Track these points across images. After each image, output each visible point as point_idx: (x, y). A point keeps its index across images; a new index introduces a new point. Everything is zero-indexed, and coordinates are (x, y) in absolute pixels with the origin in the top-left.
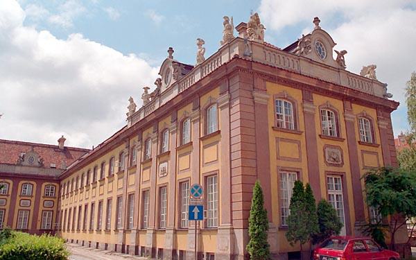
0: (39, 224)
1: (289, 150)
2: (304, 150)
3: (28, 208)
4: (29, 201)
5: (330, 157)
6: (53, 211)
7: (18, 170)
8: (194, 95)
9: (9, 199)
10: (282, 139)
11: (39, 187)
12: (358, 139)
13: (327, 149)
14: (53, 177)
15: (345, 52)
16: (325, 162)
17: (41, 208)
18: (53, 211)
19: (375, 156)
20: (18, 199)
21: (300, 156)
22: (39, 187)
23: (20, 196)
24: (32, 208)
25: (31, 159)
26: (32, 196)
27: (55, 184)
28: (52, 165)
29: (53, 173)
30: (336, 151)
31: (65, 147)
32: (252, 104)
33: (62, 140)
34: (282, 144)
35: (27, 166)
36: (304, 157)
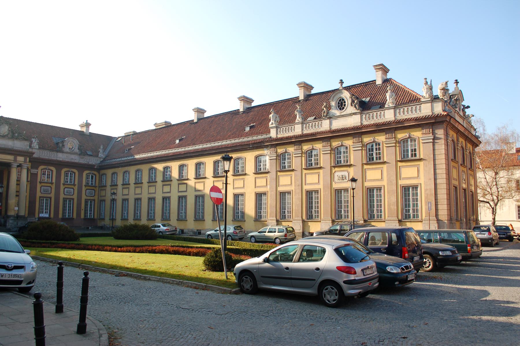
0: (83, 213)
4: (72, 190)
6: (94, 200)
7: (61, 157)
9: (54, 186)
11: (81, 176)
14: (94, 166)
15: (468, 107)
17: (84, 197)
18: (94, 200)
20: (62, 187)
22: (81, 176)
23: (64, 184)
24: (75, 197)
26: (74, 185)
27: (95, 173)
29: (93, 161)
31: (90, 133)
35: (67, 153)
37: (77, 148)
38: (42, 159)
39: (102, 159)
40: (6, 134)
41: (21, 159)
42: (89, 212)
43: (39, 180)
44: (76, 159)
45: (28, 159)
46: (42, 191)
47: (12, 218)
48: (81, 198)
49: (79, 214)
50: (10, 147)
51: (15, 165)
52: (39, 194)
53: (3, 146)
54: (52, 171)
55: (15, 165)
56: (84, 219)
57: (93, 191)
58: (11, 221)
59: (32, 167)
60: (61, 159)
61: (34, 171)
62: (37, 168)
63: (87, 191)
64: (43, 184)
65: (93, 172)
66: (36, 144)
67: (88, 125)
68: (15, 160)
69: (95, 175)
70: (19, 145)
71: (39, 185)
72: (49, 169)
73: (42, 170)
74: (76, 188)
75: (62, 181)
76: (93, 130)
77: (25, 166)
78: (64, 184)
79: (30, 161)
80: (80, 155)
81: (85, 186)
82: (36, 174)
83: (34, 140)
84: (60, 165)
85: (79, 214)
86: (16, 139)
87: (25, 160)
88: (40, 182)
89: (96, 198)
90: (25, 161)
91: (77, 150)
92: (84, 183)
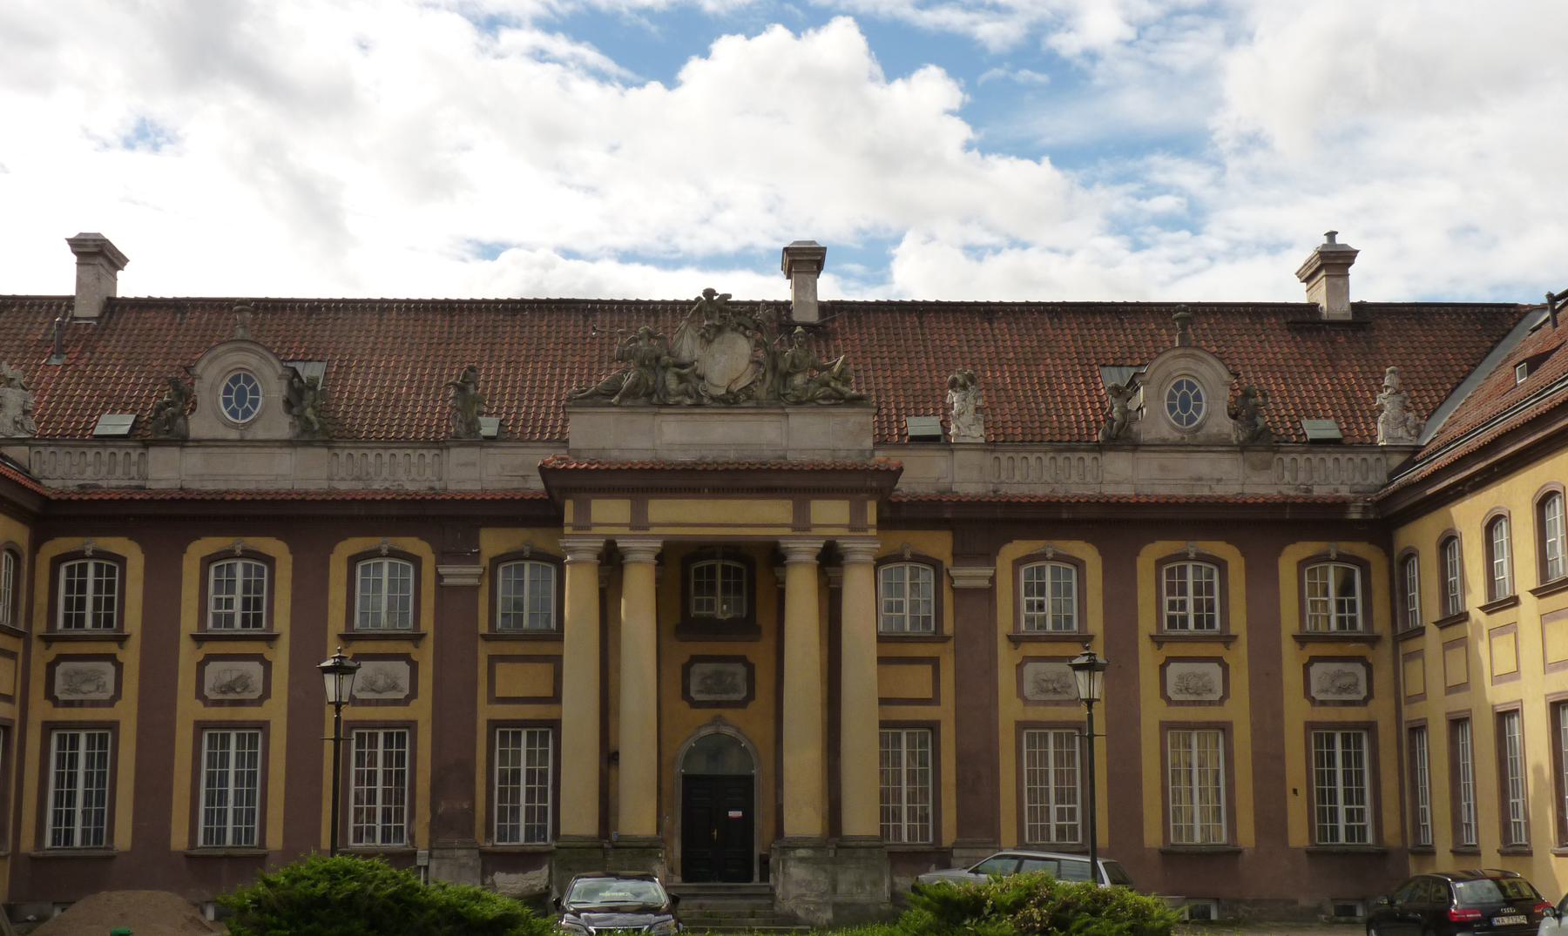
3: (1213, 714)
4: (1215, 670)
7: (1122, 477)
14: (1342, 505)
17: (1296, 712)
23: (1158, 640)
24: (1238, 711)
25: (1184, 399)
27: (1361, 549)
28: (1316, 428)
29: (1335, 479)
31: (1359, 307)
33: (1334, 261)
37: (1222, 407)
38: (1012, 504)
39: (1397, 460)
40: (743, 383)
41: (830, 514)
42: (1342, 809)
43: (1004, 625)
44: (1227, 478)
45: (872, 515)
46: (1028, 689)
47: (801, 853)
48: (1278, 715)
49: (1271, 822)
50: (768, 455)
51: (803, 552)
52: (1010, 710)
53: (732, 455)
54: (1079, 564)
55: (803, 552)
56: (1311, 854)
57: (1360, 670)
58: (797, 872)
59: (960, 557)
60: (1126, 491)
61: (971, 575)
62: (989, 558)
63: (1317, 670)
64: (1032, 649)
65: (1346, 547)
66: (968, 418)
67: (1334, 261)
68: (802, 524)
69: (1364, 565)
70: (812, 436)
71: (1006, 657)
72: (1058, 557)
73: (1018, 563)
74: (1239, 656)
75: (1147, 623)
76: (1370, 284)
77: (863, 549)
78: (1158, 640)
79: (884, 524)
80: (1243, 448)
81: (1302, 640)
82: (989, 593)
83: (954, 397)
84: (1118, 525)
85: (1271, 822)
86: (799, 403)
87: (858, 512)
88: (1016, 640)
89: (1381, 711)
90: (856, 526)
91: (1222, 424)
92: (1289, 624)
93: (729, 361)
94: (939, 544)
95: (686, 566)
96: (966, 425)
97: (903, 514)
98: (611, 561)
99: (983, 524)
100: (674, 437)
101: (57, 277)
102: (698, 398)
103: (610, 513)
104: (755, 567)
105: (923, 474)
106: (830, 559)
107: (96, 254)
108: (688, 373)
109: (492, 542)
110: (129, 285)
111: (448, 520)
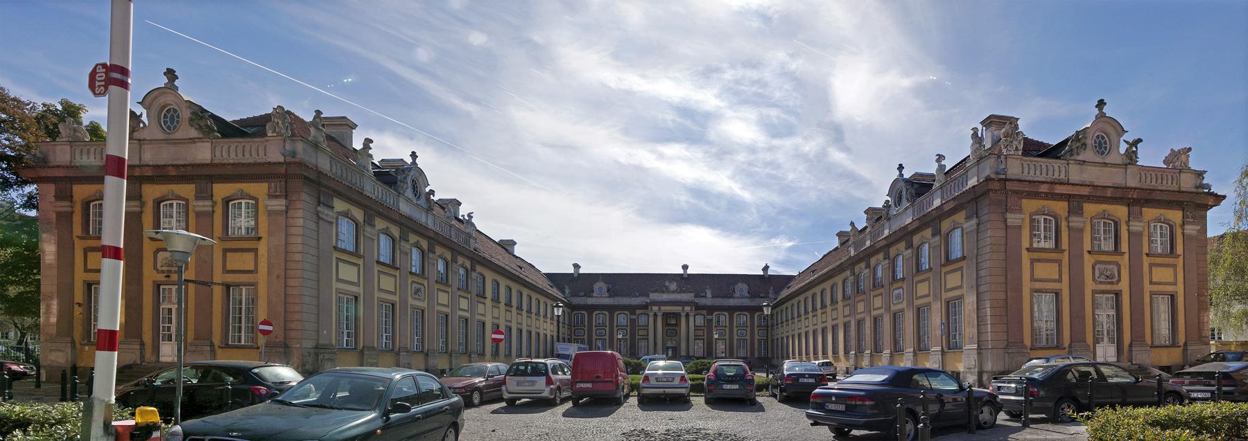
1: (1046, 271)
2: (1065, 270)
5: (1101, 274)
7: (731, 302)
8: (933, 220)
10: (1039, 261)
12: (1146, 250)
13: (1097, 267)
16: (1094, 279)
19: (1171, 270)
21: (1060, 276)
30: (1110, 267)
32: (1003, 226)
33: (766, 268)
34: (1038, 266)
36: (1065, 278)
41: (687, 308)
44: (747, 302)
51: (683, 314)
55: (683, 314)
77: (692, 314)
84: (731, 310)
93: (673, 286)
94: (705, 312)
95: (666, 316)
96: (709, 294)
97: (698, 307)
98: (655, 315)
99: (711, 309)
100: (665, 297)
101: (571, 271)
102: (667, 291)
103: (655, 308)
104: (677, 316)
105: (702, 301)
106: (687, 315)
107: (576, 266)
108: (667, 288)
109: (638, 312)
110: (581, 271)
111: (632, 309)
